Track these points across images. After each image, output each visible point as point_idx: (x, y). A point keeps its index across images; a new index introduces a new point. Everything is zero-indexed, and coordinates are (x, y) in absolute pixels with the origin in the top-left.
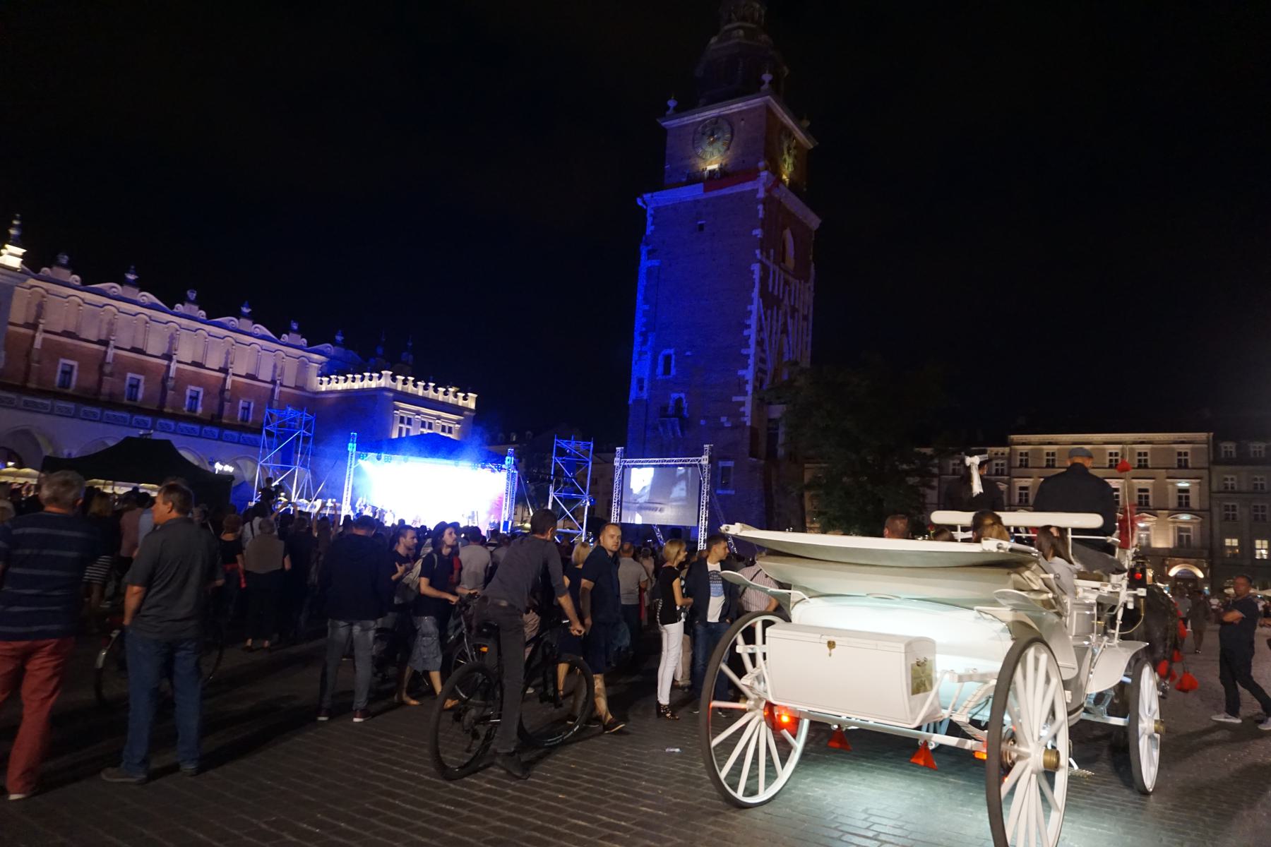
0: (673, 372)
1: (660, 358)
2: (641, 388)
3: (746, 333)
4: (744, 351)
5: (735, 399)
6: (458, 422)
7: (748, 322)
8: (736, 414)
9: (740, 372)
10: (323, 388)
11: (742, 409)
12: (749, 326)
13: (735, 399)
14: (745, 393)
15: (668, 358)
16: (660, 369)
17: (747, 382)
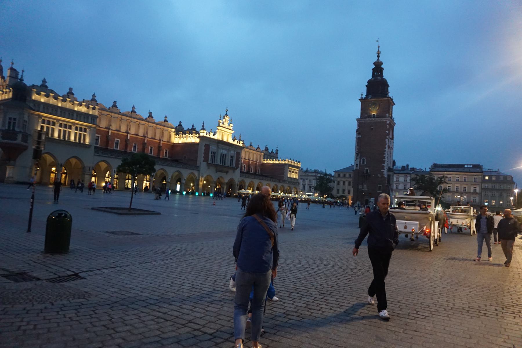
0: (365, 163)
1: (362, 160)
2: (357, 167)
3: (384, 155)
4: (384, 160)
5: (382, 170)
6: (298, 170)
7: (385, 153)
8: (382, 173)
9: (383, 164)
10: (265, 162)
11: (384, 173)
12: (385, 154)
13: (382, 170)
14: (384, 169)
15: (364, 160)
16: (362, 163)
17: (385, 167)
